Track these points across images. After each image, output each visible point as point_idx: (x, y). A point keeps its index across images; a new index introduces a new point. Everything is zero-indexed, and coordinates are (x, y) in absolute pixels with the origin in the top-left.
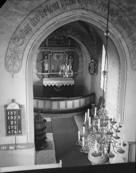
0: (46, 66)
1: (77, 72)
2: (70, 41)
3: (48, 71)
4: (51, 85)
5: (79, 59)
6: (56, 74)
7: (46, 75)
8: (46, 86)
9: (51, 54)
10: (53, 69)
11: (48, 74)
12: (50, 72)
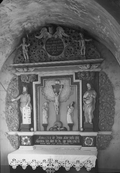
0: (26, 111)
1: (110, 130)
2: (83, 41)
3: (32, 125)
4: (29, 167)
5: (113, 95)
6: (52, 136)
7: (27, 138)
8: (14, 167)
9: (39, 82)
10: (44, 121)
11: (31, 134)
12: (37, 130)
